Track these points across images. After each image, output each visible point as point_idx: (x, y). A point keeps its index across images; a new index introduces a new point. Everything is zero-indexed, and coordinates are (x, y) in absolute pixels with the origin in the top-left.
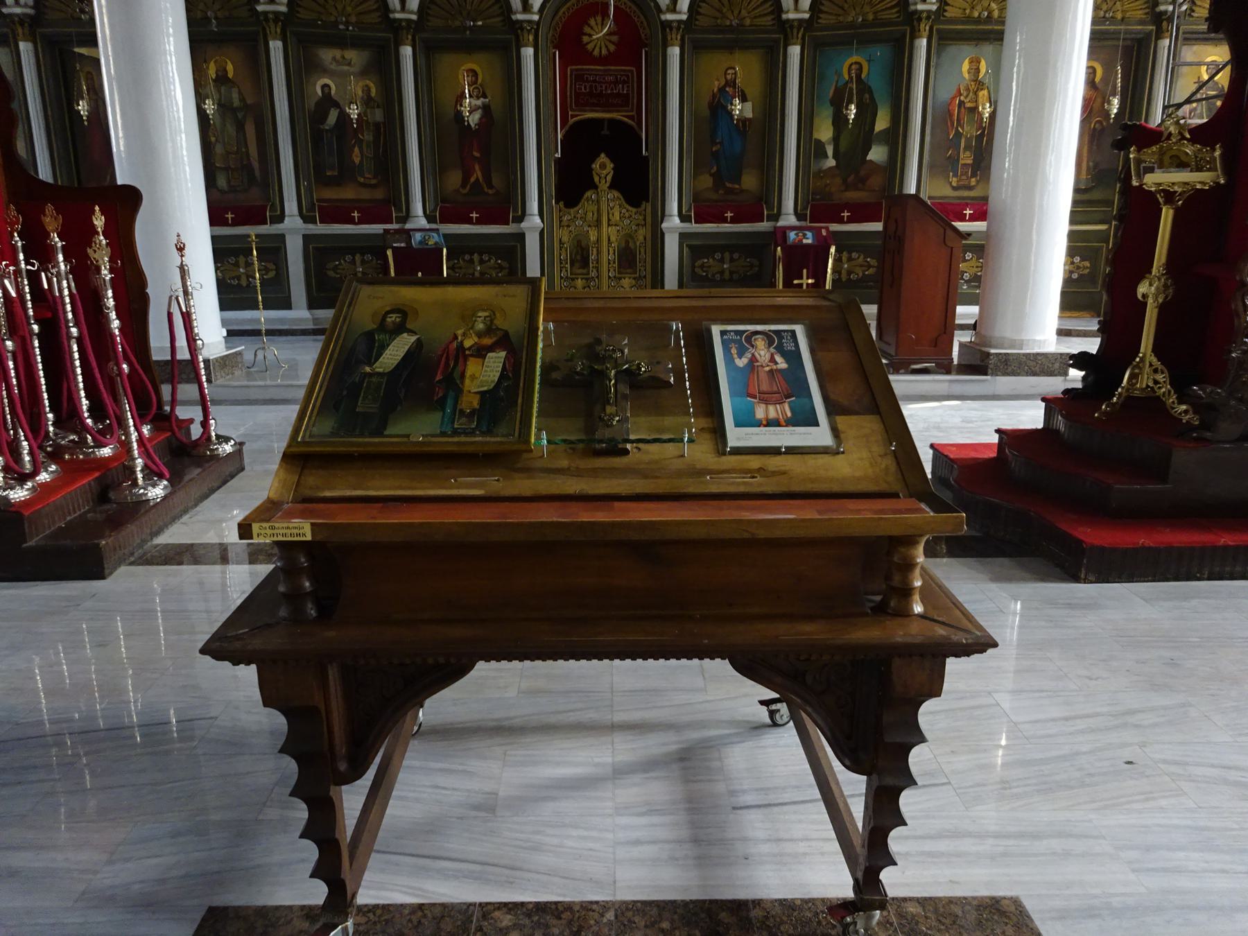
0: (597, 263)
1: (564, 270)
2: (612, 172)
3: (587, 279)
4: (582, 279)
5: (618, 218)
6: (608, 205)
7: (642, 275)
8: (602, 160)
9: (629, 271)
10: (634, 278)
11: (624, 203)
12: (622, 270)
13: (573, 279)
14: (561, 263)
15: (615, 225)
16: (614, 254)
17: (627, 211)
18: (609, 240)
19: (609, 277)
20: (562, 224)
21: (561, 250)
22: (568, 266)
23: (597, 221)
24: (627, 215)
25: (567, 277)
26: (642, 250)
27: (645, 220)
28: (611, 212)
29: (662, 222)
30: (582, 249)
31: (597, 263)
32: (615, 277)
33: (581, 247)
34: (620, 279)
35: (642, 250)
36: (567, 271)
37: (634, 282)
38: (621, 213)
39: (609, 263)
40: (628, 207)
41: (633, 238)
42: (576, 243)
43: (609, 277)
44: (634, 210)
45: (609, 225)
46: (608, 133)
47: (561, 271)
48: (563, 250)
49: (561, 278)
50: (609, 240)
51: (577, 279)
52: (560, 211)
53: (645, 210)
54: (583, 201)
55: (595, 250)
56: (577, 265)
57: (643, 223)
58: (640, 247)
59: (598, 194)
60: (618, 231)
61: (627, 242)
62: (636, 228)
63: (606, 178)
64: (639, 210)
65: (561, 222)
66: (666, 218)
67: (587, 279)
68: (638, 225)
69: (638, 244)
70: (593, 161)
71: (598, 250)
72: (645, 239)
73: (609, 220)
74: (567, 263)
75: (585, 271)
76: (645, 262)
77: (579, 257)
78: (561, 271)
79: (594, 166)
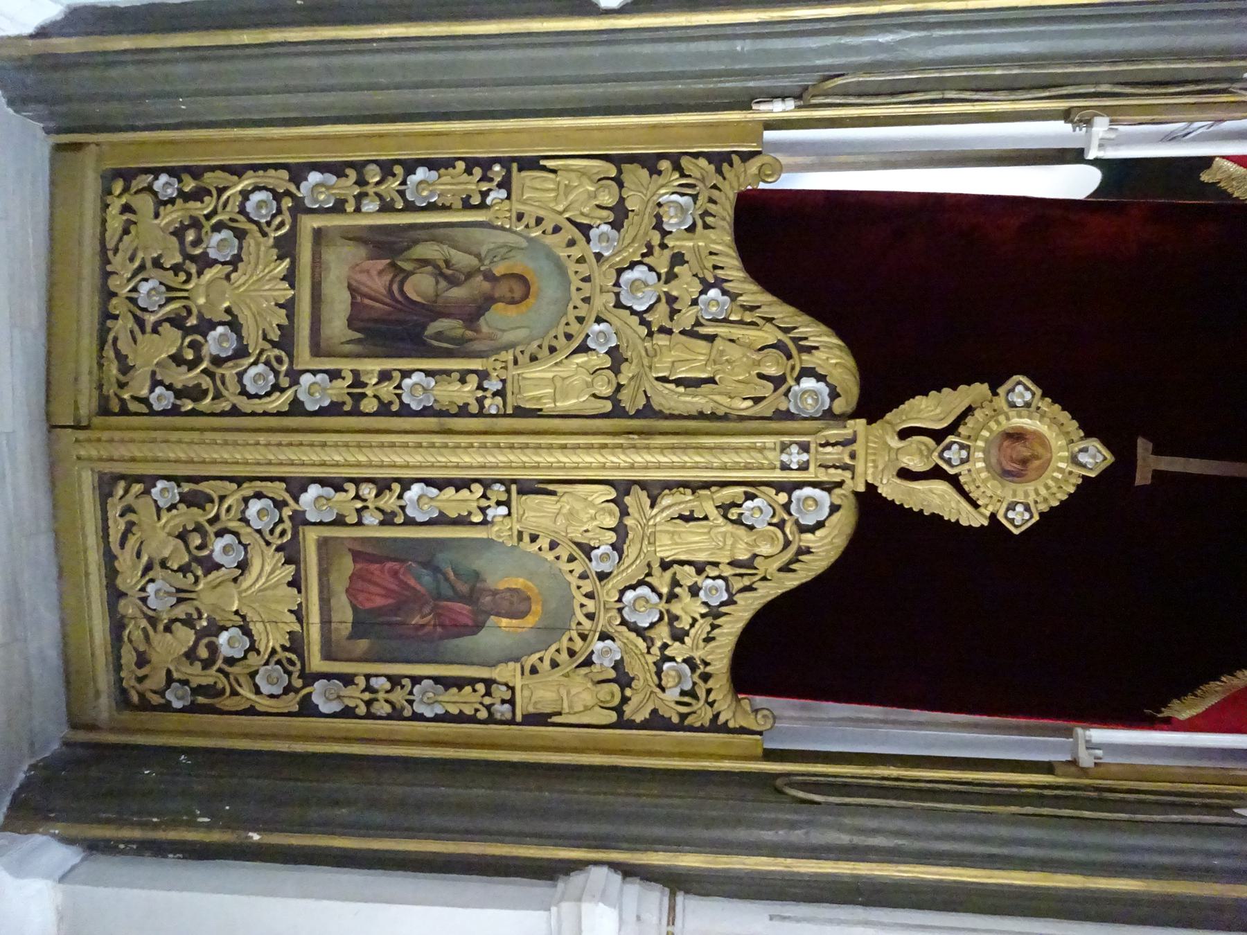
0: (384, 409)
1: (347, 186)
2: (974, 519)
3: (286, 341)
4: (289, 306)
5: (668, 554)
6: (752, 488)
7: (319, 693)
8: (1056, 442)
9: (344, 614)
10: (296, 644)
11: (767, 593)
12: (347, 566)
13: (286, 247)
14: (386, 168)
15: (621, 531)
16: (442, 520)
17: (714, 614)
18: (528, 488)
19: (297, 486)
20: (636, 175)
21: (471, 164)
22: (370, 216)
23: (648, 411)
24: (687, 608)
25: (300, 208)
26: (466, 700)
27: (656, 721)
28: (707, 504)
29: (628, 872)
30: (473, 313)
31: (384, 409)
32: (299, 520)
33: (486, 303)
34: (291, 554)
35: (466, 700)
36: (338, 207)
37: (271, 638)
38: (700, 569)
39: (383, 486)
40: (746, 608)
41: (551, 630)
42: (518, 264)
43: (297, 486)
44: (720, 657)
45: (623, 488)
46: (1142, 477)
47: (337, 170)
48: (471, 184)
49: (297, 173)
50: (528, 488)
51: (290, 278)
52: (720, 160)
53: (715, 726)
54: (784, 313)
55: (466, 393)
56: (377, 282)
57: (638, 710)
58: (489, 683)
59: (829, 415)
60: (587, 550)
61: (517, 605)
62: (604, 666)
63: (936, 473)
64: (721, 685)
65: (650, 163)
66: (655, 897)
67: (286, 341)
68: (623, 679)
69: (505, 673)
70: (1052, 390)
71: (463, 411)
72: (539, 719)
73: (655, 490)
74: (387, 207)
75: (337, 325)
76: (396, 714)
77: (421, 286)
78: (337, 170)
79: (1021, 390)
